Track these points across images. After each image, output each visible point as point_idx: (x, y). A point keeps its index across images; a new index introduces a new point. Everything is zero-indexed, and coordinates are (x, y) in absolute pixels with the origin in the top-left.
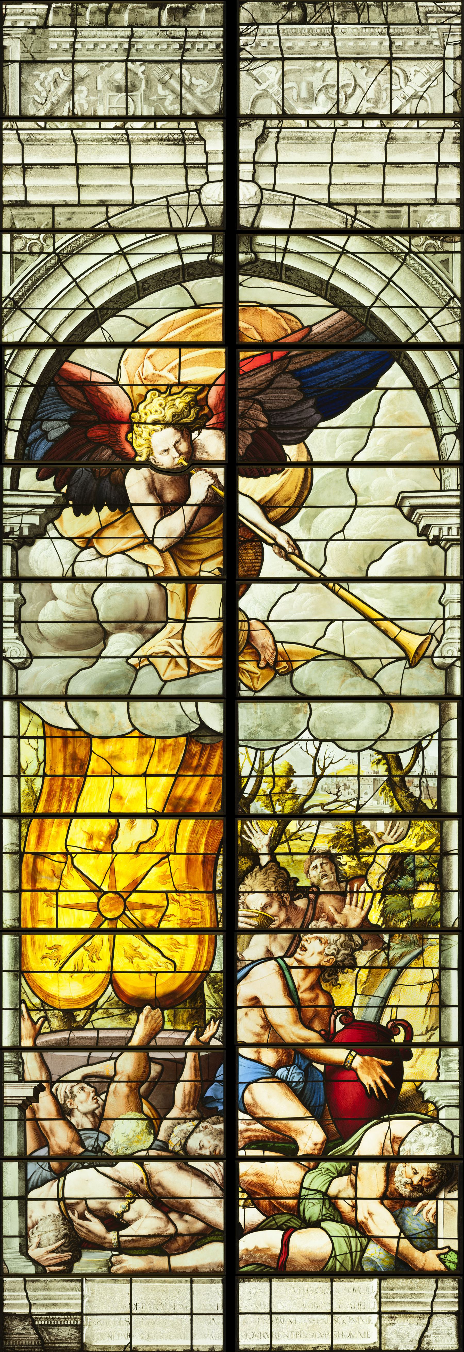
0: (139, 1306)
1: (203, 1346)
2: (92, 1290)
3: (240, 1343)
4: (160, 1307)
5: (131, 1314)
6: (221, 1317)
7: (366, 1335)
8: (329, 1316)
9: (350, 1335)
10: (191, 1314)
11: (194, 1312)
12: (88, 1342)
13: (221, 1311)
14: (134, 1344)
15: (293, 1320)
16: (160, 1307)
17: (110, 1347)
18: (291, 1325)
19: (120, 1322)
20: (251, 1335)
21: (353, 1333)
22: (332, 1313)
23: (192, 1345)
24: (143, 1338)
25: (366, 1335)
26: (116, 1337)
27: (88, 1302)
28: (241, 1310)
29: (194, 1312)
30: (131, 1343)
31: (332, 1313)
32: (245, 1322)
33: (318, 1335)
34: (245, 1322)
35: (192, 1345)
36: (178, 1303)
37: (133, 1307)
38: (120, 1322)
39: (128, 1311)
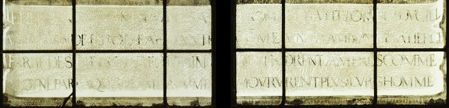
0: (87, 39)
1: (182, 99)
2: (16, 14)
3: (238, 95)
4: (117, 41)
5: (74, 51)
6: (209, 56)
7: (427, 82)
8: (371, 54)
9: (403, 82)
10: (165, 51)
11: (169, 47)
12: (10, 93)
13: (209, 46)
14: (79, 95)
15: (317, 60)
16: (117, 41)
17: (42, 99)
18: (314, 68)
19: (58, 63)
20: (253, 82)
21: (407, 79)
22: (375, 50)
23: (165, 98)
24: (92, 87)
25: (427, 82)
26: (52, 86)
27: (10, 33)
28: (240, 44)
29: (169, 47)
30: (74, 93)
31: (375, 50)
32: (245, 62)
33: (355, 82)
34: (245, 62)
35: (165, 98)
36: (145, 34)
37: (78, 40)
38: (58, 63)
39: (69, 46)
